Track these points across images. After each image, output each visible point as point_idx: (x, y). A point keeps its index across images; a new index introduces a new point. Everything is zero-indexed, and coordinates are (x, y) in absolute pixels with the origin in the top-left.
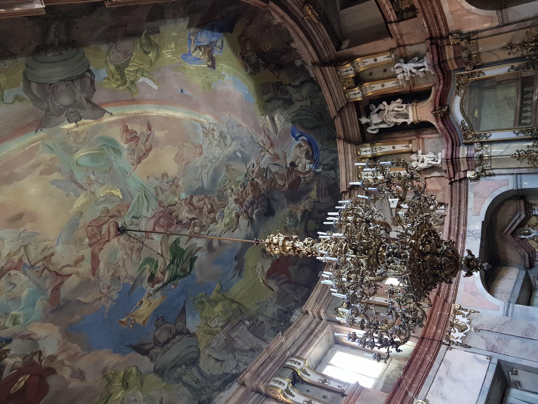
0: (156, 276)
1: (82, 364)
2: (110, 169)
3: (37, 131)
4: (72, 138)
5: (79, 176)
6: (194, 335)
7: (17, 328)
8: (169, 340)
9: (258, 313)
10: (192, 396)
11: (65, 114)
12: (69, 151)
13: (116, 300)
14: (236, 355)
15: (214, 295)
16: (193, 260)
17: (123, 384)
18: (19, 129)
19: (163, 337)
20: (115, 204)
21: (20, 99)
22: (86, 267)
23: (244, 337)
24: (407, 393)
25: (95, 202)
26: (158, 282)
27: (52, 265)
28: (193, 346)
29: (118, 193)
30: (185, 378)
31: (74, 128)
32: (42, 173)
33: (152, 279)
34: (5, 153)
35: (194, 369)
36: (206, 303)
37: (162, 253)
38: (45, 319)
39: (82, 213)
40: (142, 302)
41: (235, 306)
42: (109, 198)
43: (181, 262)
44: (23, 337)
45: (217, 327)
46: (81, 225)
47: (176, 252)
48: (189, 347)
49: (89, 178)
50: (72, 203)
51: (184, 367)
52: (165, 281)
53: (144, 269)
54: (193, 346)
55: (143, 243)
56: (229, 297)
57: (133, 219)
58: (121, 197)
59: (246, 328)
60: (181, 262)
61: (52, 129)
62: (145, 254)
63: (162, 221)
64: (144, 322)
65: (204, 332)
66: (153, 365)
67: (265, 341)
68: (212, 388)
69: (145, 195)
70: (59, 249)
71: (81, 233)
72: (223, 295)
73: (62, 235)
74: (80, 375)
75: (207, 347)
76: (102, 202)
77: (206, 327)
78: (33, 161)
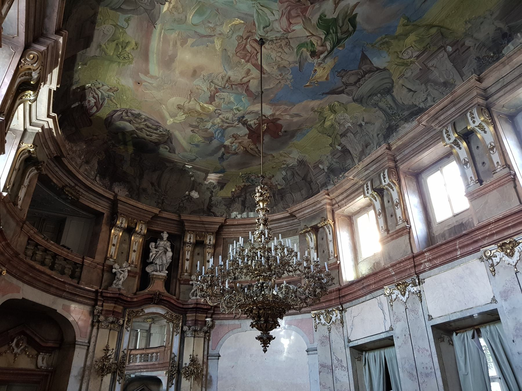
0: (317, 51)
1: (294, 110)
2: (217, 10)
3: (155, 27)
4: (175, 13)
5: (202, 31)
6: (385, 69)
7: (242, 112)
8: (359, 80)
9: (466, 35)
10: (385, 119)
11: (156, 3)
12: (181, 21)
13: (293, 78)
14: (428, 87)
15: (399, 30)
16: (352, 20)
17: (332, 111)
18: (148, 35)
19: (353, 79)
20: (243, 29)
21: (129, 19)
22: (255, 73)
23: (442, 66)
24: (456, 250)
25: (227, 37)
26: (322, 53)
27: (234, 82)
28: (386, 78)
29: (238, 21)
30: (380, 104)
31: (169, 6)
32: (182, 45)
33: (313, 54)
34: (155, 50)
35: (389, 97)
36: (392, 41)
37: (311, 33)
38: (254, 104)
39: (225, 49)
40: (316, 70)
41: (434, 31)
42: (234, 29)
43: (338, 28)
44: (249, 113)
45: (410, 58)
46: (231, 56)
47: (327, 25)
48: (382, 79)
49: (209, 27)
50: (214, 48)
51: (379, 95)
52: (329, 48)
53: (302, 53)
54: (386, 78)
55: (287, 38)
56: (424, 23)
57: (265, 29)
58: (242, 22)
59: (446, 56)
60: (338, 28)
61: (160, 19)
62: (294, 45)
63: (293, 13)
64: (326, 79)
65: (396, 64)
66: (351, 97)
67: (462, 75)
68: (401, 116)
69: (262, 6)
70: (230, 73)
71: (236, 59)
72: (413, 25)
73: (225, 66)
74: (297, 115)
75: (402, 76)
76: (232, 34)
77: (398, 60)
78: (171, 43)
